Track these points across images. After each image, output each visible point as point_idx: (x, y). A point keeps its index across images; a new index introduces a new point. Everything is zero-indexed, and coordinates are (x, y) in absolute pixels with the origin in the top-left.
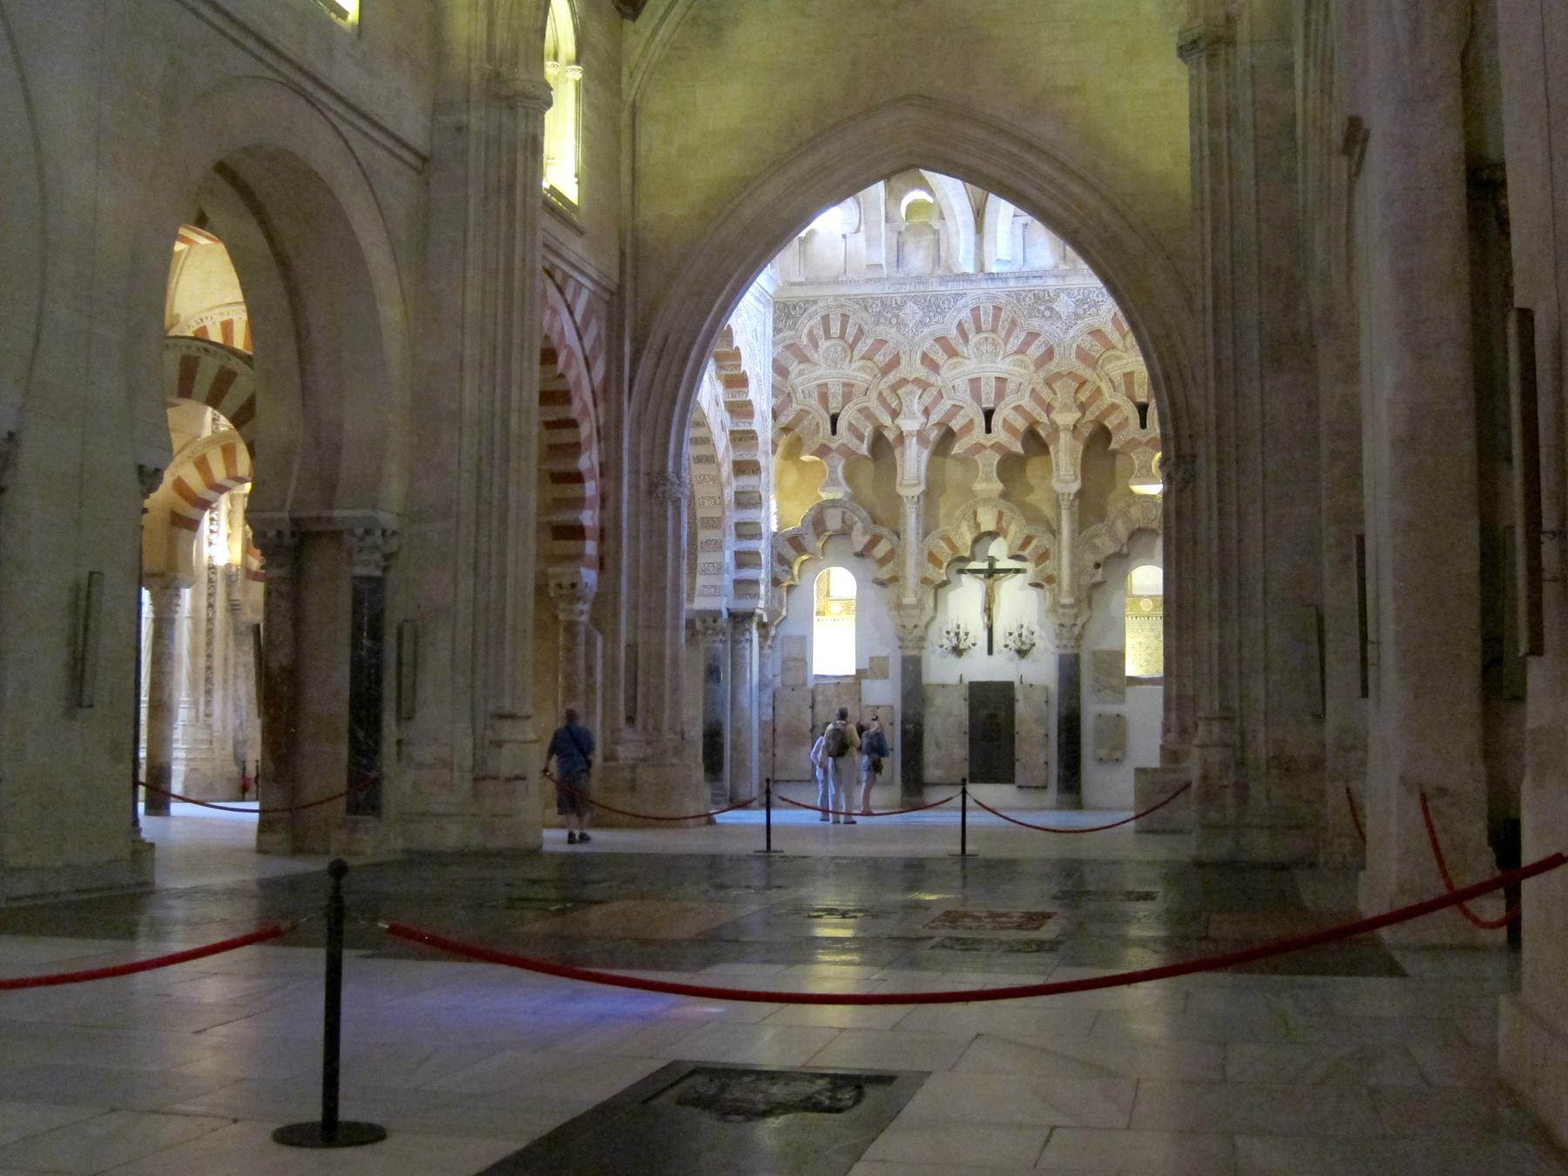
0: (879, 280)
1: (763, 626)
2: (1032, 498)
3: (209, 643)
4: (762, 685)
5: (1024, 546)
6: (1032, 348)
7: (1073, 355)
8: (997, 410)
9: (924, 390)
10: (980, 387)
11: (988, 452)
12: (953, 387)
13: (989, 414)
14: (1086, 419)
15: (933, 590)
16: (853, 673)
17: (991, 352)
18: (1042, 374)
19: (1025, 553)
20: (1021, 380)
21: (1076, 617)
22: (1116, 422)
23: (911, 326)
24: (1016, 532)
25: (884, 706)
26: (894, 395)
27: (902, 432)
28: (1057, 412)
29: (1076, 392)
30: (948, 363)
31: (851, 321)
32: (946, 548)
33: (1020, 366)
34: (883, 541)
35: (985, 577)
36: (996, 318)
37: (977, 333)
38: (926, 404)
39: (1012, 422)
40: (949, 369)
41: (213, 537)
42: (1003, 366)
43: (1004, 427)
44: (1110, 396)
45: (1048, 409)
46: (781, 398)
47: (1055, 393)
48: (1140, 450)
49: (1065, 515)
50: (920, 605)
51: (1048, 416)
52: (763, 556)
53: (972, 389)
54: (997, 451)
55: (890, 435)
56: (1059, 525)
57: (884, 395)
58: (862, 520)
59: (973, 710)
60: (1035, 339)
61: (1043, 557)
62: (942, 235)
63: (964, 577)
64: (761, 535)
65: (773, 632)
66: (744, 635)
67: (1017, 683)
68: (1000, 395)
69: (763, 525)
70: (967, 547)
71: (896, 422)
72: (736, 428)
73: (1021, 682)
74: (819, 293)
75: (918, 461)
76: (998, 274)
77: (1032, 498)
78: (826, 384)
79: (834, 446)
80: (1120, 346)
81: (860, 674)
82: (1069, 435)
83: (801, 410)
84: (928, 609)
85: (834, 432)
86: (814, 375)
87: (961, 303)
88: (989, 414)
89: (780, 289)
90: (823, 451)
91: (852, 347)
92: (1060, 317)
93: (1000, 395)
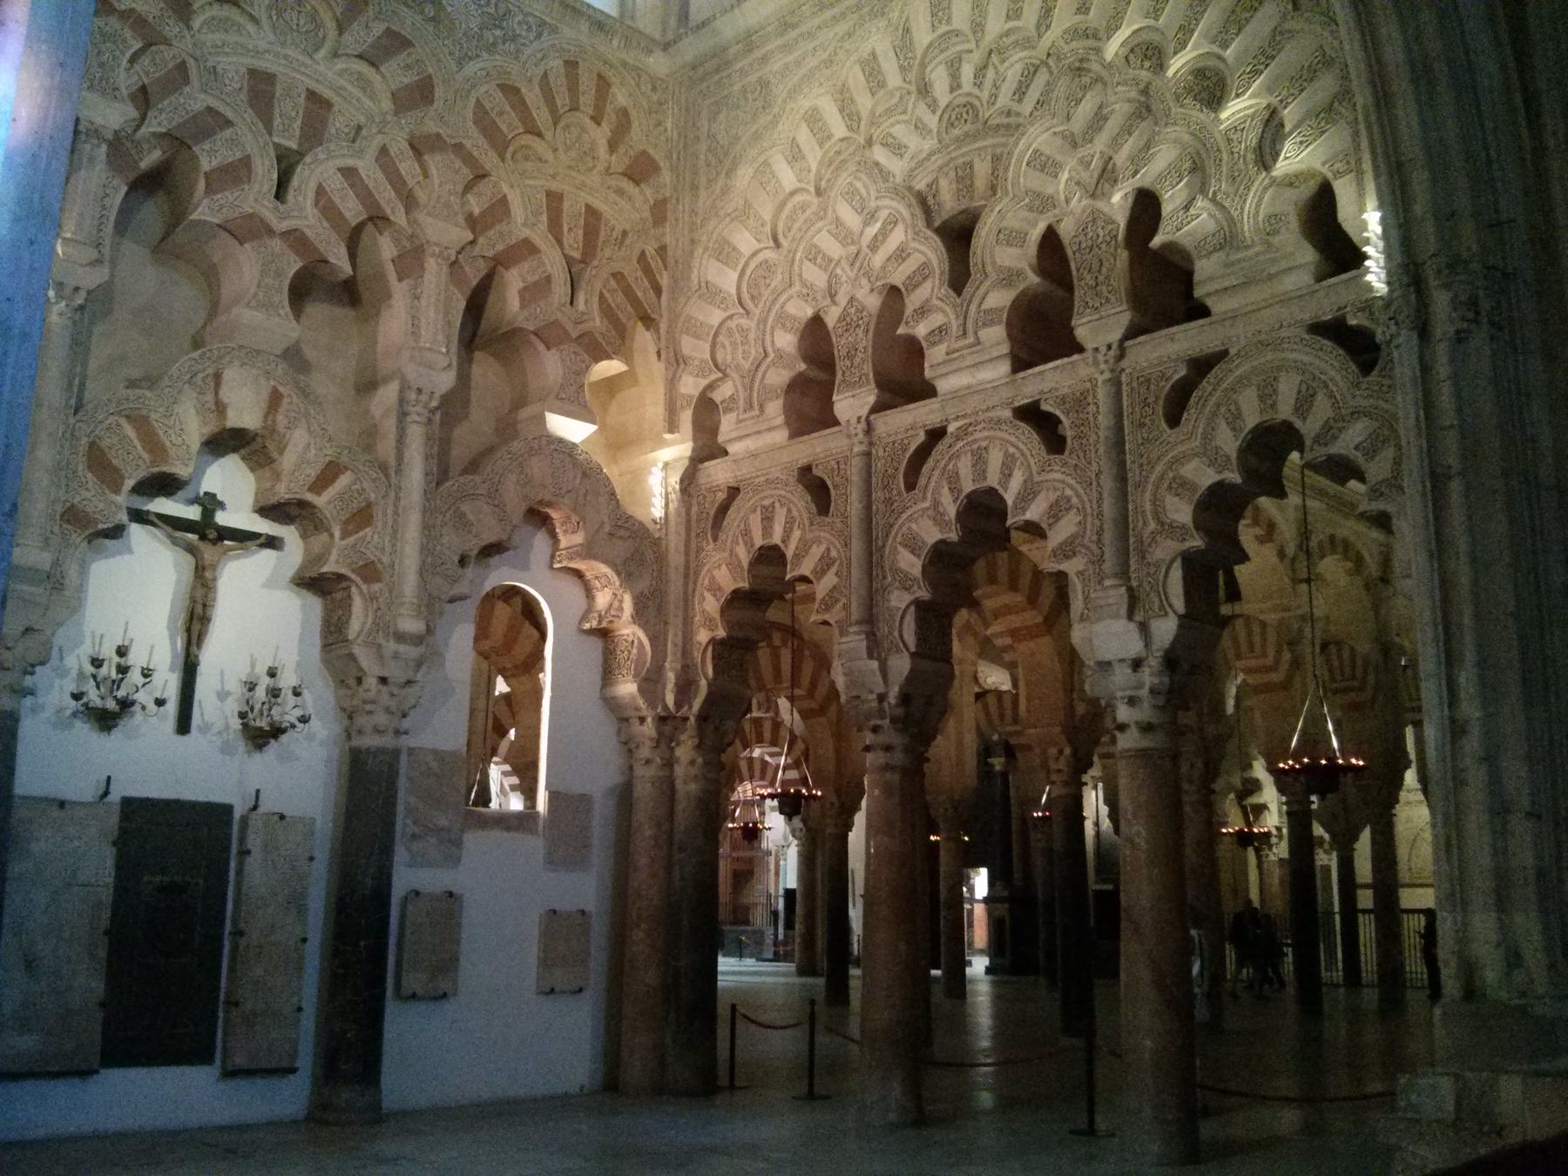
7: (470, 114)
8: (308, 159)
11: (276, 244)
14: (477, 251)
19: (320, 501)
20: (363, 120)
21: (419, 664)
22: (531, 279)
28: (429, 214)
29: (468, 188)
33: (364, 89)
35: (203, 537)
39: (337, 200)
44: (525, 225)
45: (409, 202)
47: (426, 175)
48: (566, 347)
50: (54, 580)
51: (407, 213)
54: (297, 253)
59: (127, 867)
61: (361, 517)
63: (136, 530)
80: (548, 135)
82: (445, 269)
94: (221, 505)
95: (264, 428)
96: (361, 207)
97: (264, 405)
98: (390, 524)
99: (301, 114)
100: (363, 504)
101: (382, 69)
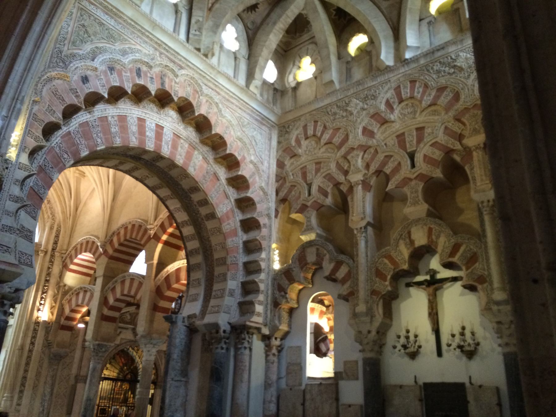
0: (333, 92)
1: (266, 339)
2: (462, 219)
3: (27, 364)
4: (267, 385)
5: (453, 253)
6: (442, 98)
8: (418, 149)
9: (365, 152)
10: (405, 139)
12: (386, 144)
13: (412, 156)
15: (381, 300)
16: (332, 375)
17: (411, 112)
18: (451, 113)
19: (455, 259)
23: (355, 114)
24: (445, 243)
25: (356, 405)
26: (346, 161)
27: (351, 183)
28: (468, 137)
30: (381, 130)
31: (319, 123)
32: (390, 265)
33: (435, 115)
34: (344, 264)
36: (412, 89)
37: (400, 103)
38: (367, 161)
40: (383, 133)
41: (41, 307)
42: (421, 119)
43: (424, 161)
46: (281, 182)
47: (464, 124)
49: (487, 218)
50: (370, 313)
51: (461, 143)
52: (262, 286)
53: (399, 142)
55: (344, 188)
56: (484, 231)
57: (340, 162)
58: (328, 252)
60: (443, 92)
61: (472, 260)
62: (374, 53)
63: (413, 291)
64: (261, 270)
65: (276, 343)
66: (243, 343)
67: (468, 384)
68: (420, 140)
69: (263, 265)
70: (405, 262)
71: (347, 178)
72: (239, 197)
73: (471, 383)
74: (302, 113)
75: (363, 202)
76: (411, 59)
77: (462, 219)
78: (306, 166)
79: (309, 204)
81: (338, 375)
83: (291, 186)
84: (377, 316)
85: (310, 194)
86: (299, 163)
87: (386, 88)
88: (412, 156)
89: (280, 118)
90: (303, 209)
91: (320, 139)
92: (461, 69)
93: (420, 140)
94: (439, 272)
95: (428, 242)
96: (441, 152)
97: (426, 234)
98: (485, 258)
99: (415, 137)
100: (472, 254)
101: (438, 103)
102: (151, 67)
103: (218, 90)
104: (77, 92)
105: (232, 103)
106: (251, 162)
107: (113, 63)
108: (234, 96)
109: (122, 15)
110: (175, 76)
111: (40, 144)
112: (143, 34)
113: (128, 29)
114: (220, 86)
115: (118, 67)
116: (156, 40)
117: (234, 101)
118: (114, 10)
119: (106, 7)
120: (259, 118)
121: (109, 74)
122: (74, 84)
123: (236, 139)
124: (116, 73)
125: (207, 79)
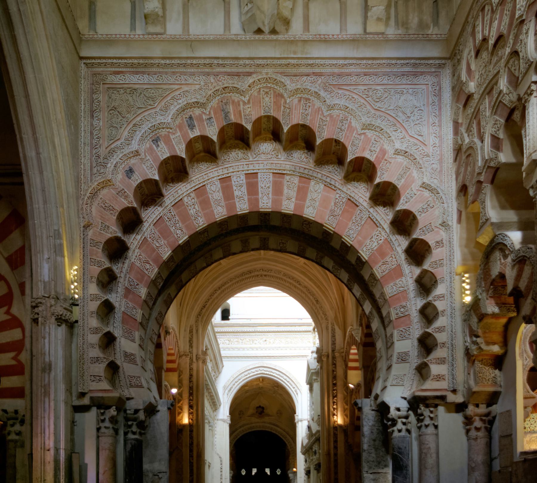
102: (202, 105)
103: (317, 70)
104: (125, 192)
105: (349, 75)
106: (397, 152)
107: (157, 132)
108: (347, 62)
109: (152, 62)
110: (241, 95)
111: (103, 268)
112: (185, 65)
113: (166, 73)
114: (318, 61)
115: (163, 132)
116: (202, 62)
117: (352, 69)
118: (141, 61)
119: (132, 65)
120: (407, 69)
121: (155, 148)
122: (120, 185)
123: (362, 129)
124: (162, 143)
125: (294, 65)
